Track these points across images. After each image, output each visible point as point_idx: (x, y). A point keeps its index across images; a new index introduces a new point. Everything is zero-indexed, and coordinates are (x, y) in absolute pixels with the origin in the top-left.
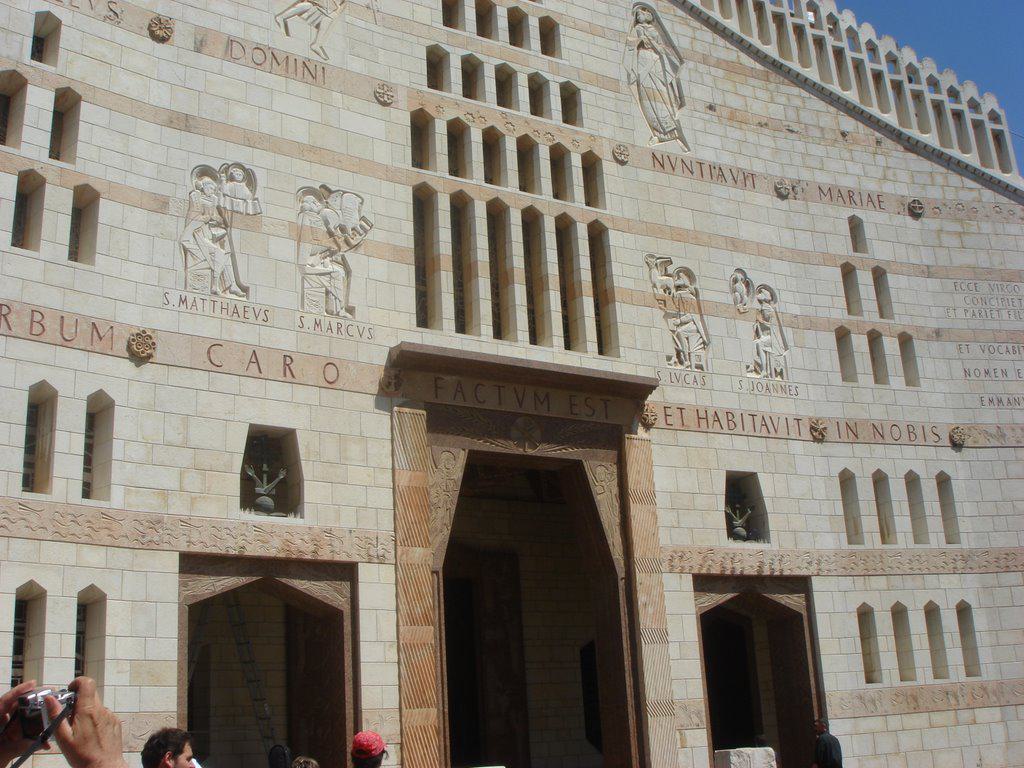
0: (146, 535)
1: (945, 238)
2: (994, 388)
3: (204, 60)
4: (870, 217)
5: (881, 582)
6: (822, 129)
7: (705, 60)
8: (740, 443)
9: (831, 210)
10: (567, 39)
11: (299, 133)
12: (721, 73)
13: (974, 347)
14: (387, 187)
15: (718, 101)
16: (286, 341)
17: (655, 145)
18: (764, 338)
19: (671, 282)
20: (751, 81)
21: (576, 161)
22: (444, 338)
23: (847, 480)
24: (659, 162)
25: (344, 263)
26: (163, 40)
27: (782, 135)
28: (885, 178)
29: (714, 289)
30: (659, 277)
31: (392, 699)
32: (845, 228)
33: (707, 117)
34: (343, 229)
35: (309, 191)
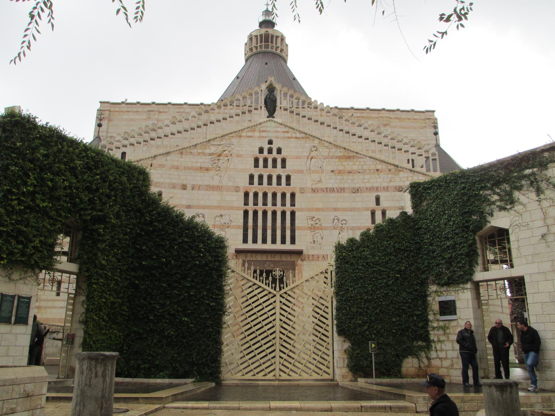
3: (195, 192)
4: (383, 195)
6: (370, 170)
7: (332, 158)
9: (369, 194)
10: (287, 163)
11: (216, 204)
12: (337, 160)
14: (237, 212)
15: (335, 168)
17: (314, 186)
18: (343, 234)
19: (313, 223)
21: (288, 196)
22: (250, 246)
24: (314, 191)
25: (225, 231)
26: (185, 189)
27: (356, 174)
28: (391, 181)
29: (326, 223)
30: (311, 222)
32: (374, 199)
33: (331, 174)
34: (225, 223)
35: (217, 216)
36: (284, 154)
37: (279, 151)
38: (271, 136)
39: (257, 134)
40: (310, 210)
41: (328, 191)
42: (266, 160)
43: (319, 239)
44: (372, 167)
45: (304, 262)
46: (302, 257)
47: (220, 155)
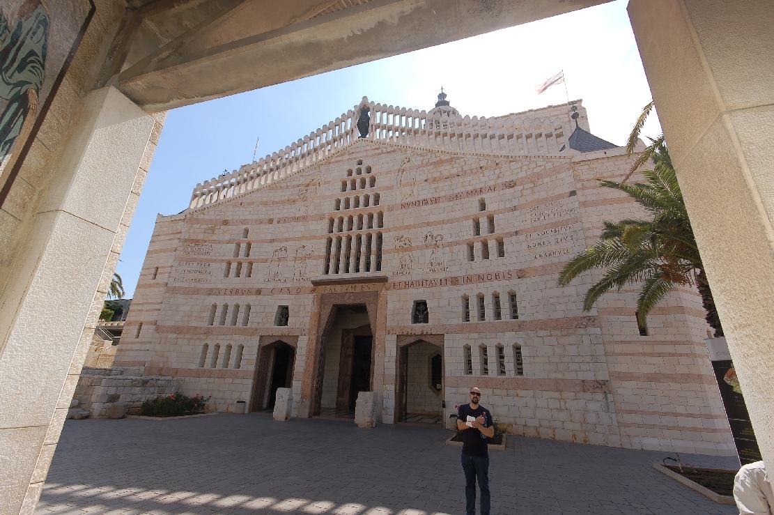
0: (253, 332)
1: (525, 193)
2: (539, 250)
4: (487, 197)
5: (476, 335)
7: (427, 165)
8: (421, 290)
13: (534, 235)
16: (288, 285)
19: (402, 244)
20: (445, 164)
22: (332, 276)
23: (466, 299)
28: (499, 177)
30: (398, 243)
31: (302, 370)
36: (373, 172)
37: (369, 170)
38: (359, 156)
39: (346, 157)
40: (396, 229)
41: (421, 203)
42: (354, 183)
43: (408, 262)
44: (474, 166)
45: (389, 292)
46: (387, 285)
47: (308, 185)
